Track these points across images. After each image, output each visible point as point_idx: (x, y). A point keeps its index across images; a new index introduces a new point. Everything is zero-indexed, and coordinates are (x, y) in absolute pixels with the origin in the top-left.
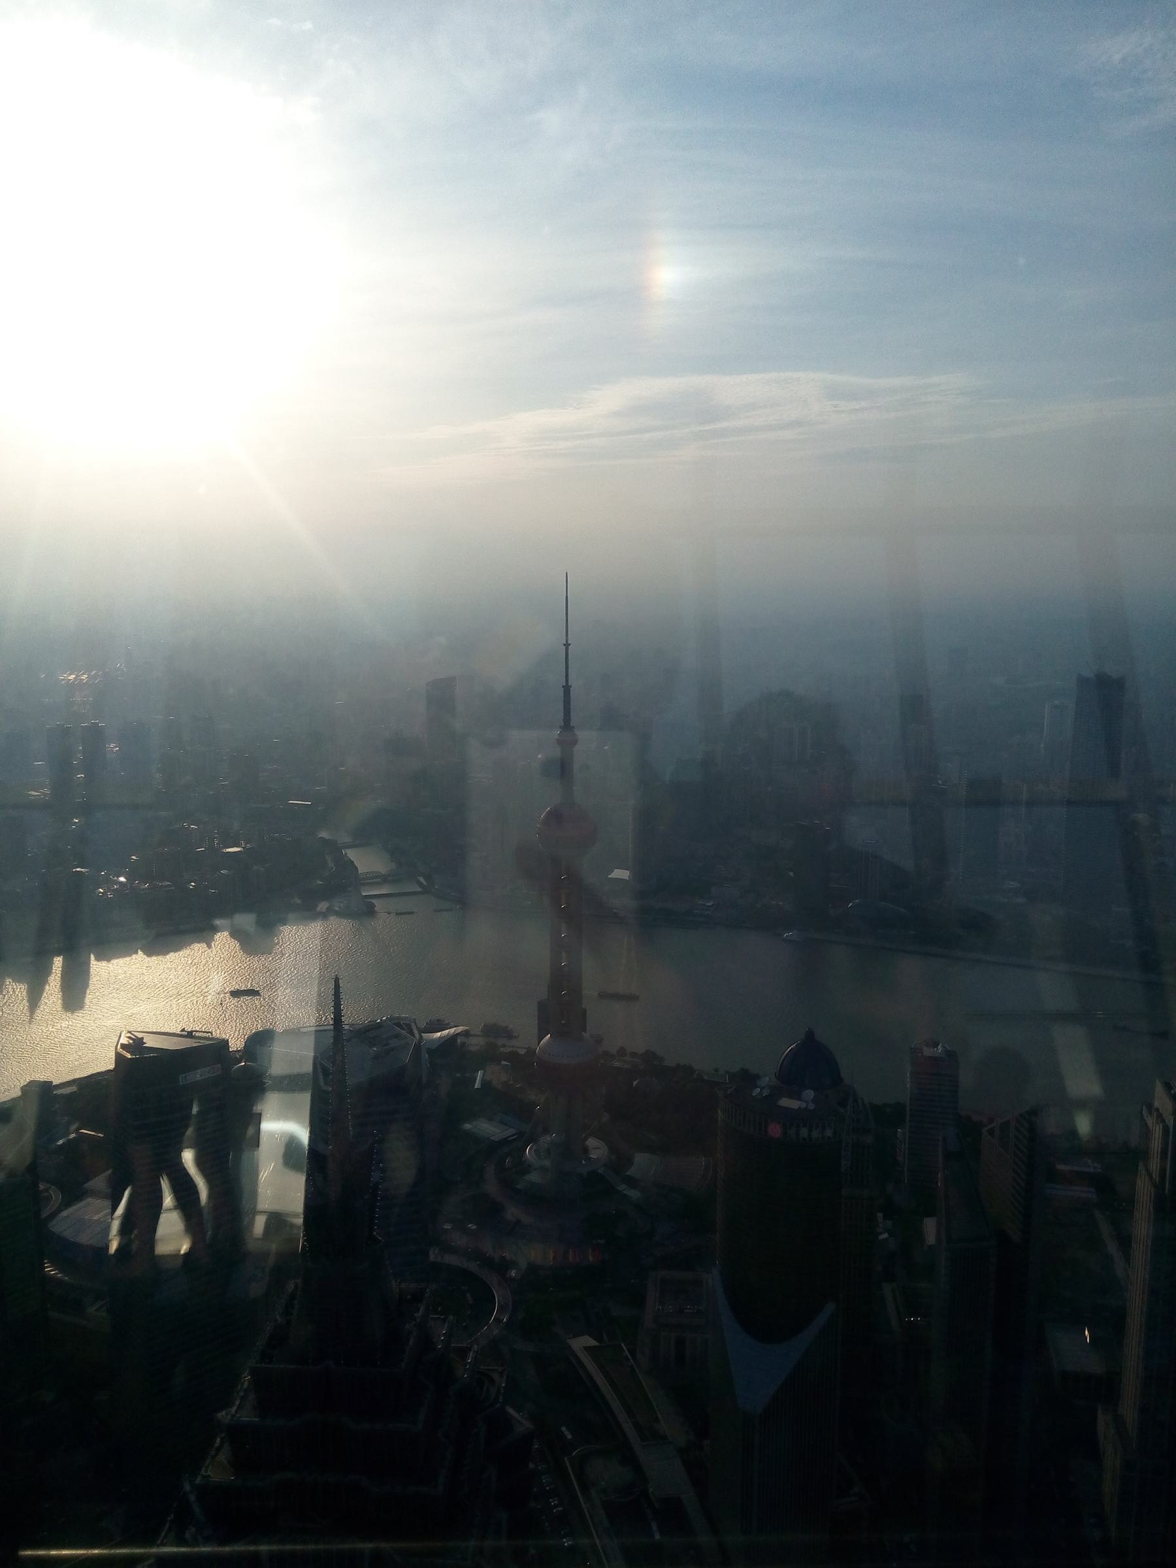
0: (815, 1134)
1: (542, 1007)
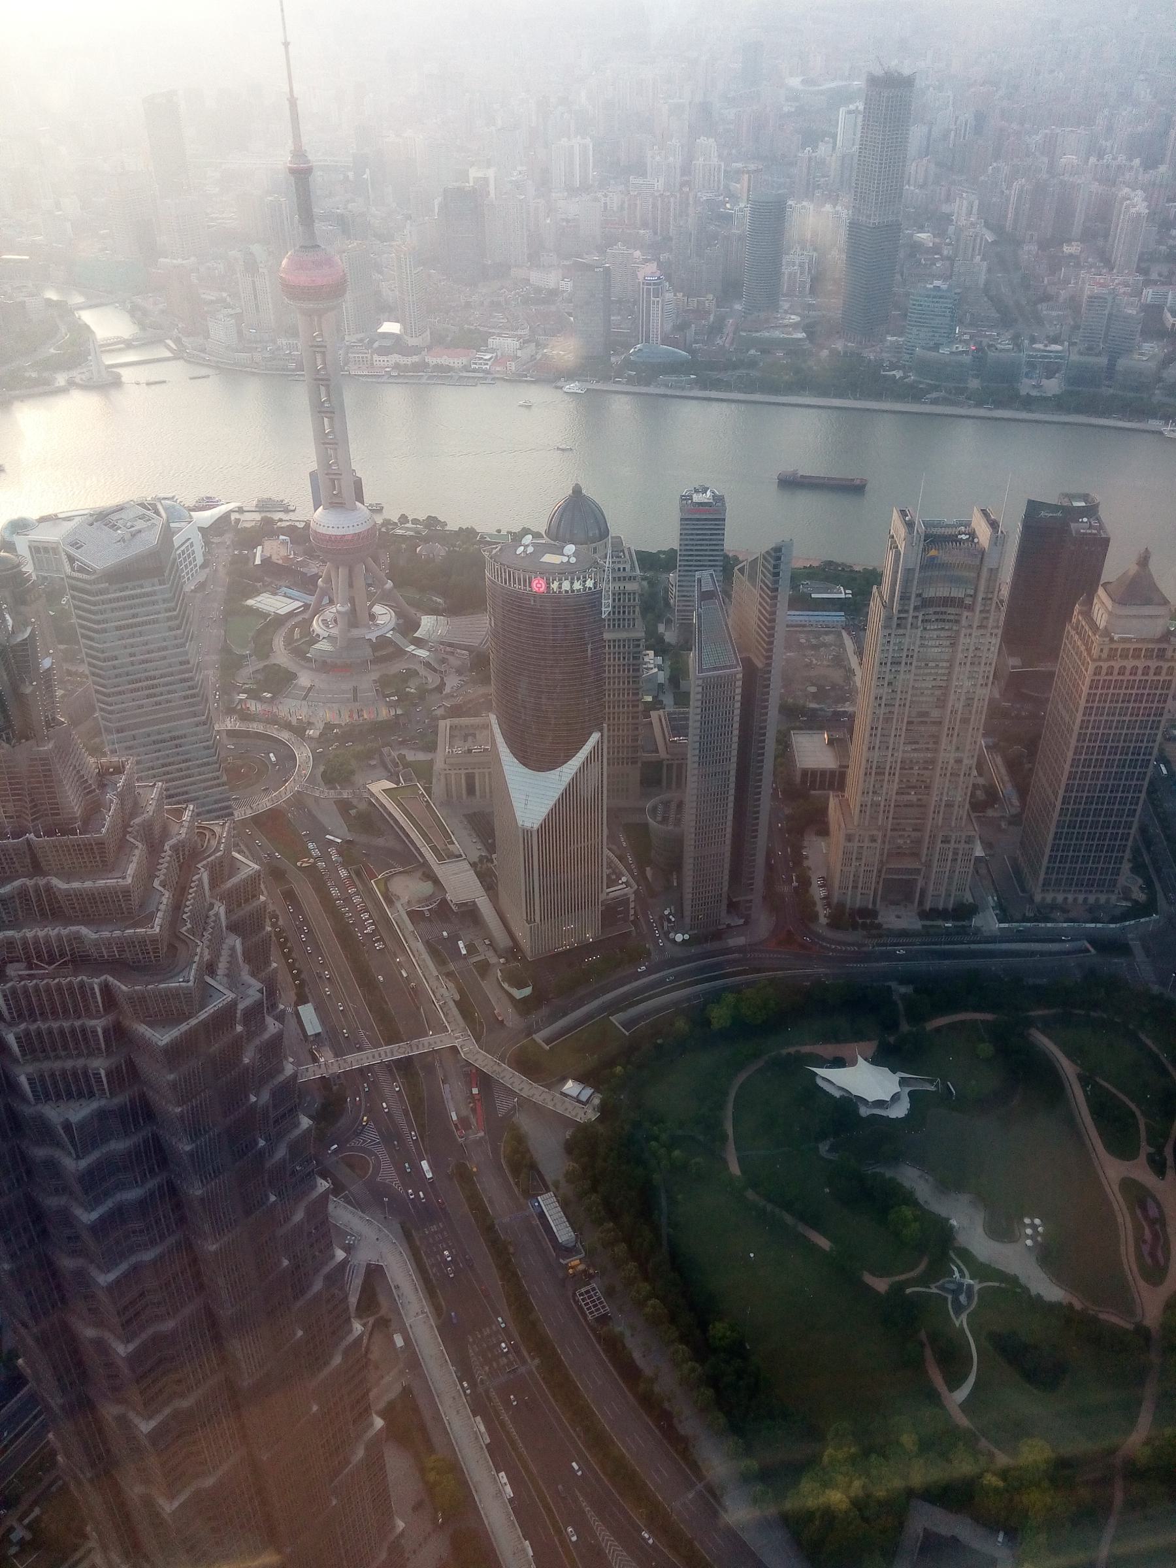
0: (577, 586)
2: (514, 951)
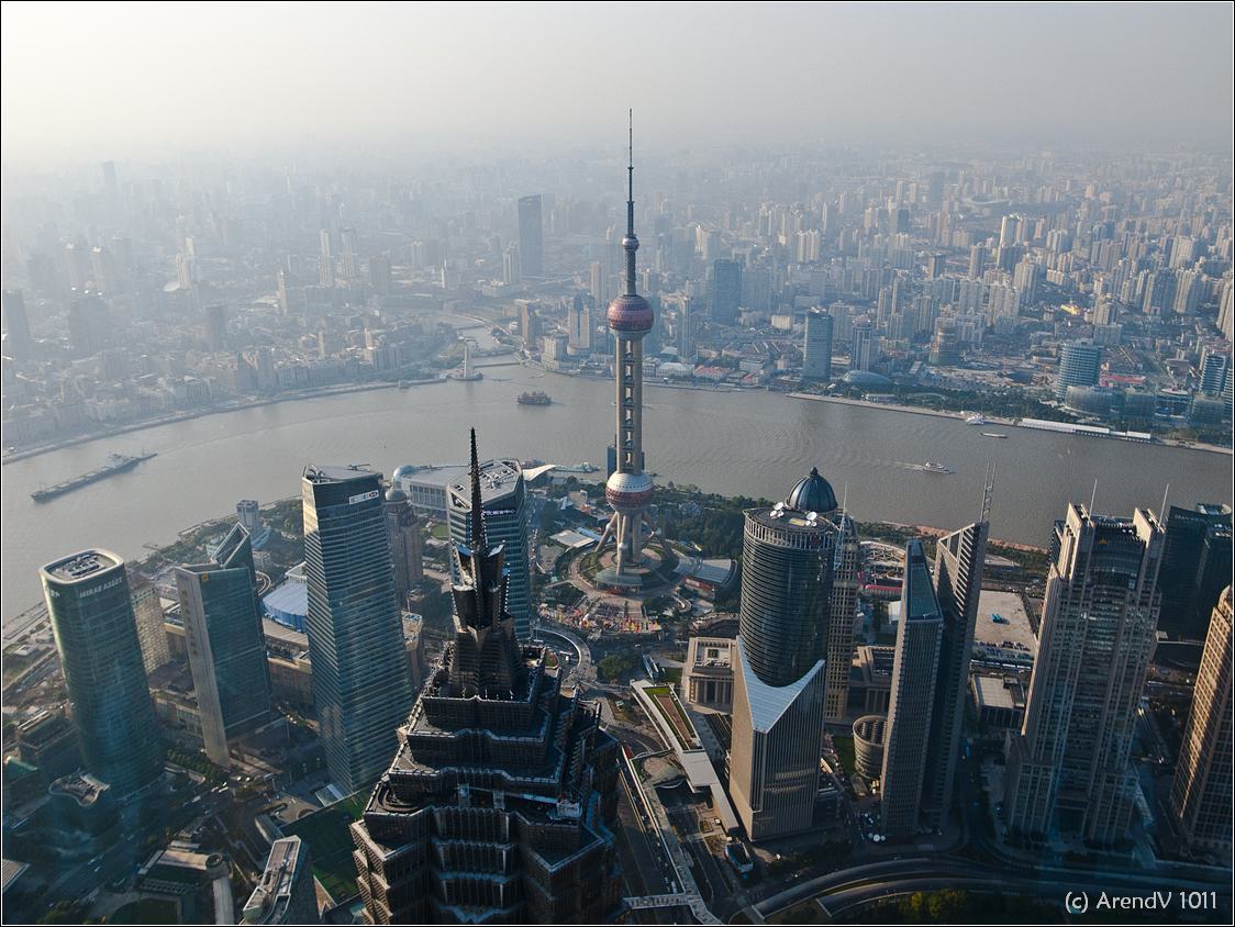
1: (611, 452)
2: (738, 832)
